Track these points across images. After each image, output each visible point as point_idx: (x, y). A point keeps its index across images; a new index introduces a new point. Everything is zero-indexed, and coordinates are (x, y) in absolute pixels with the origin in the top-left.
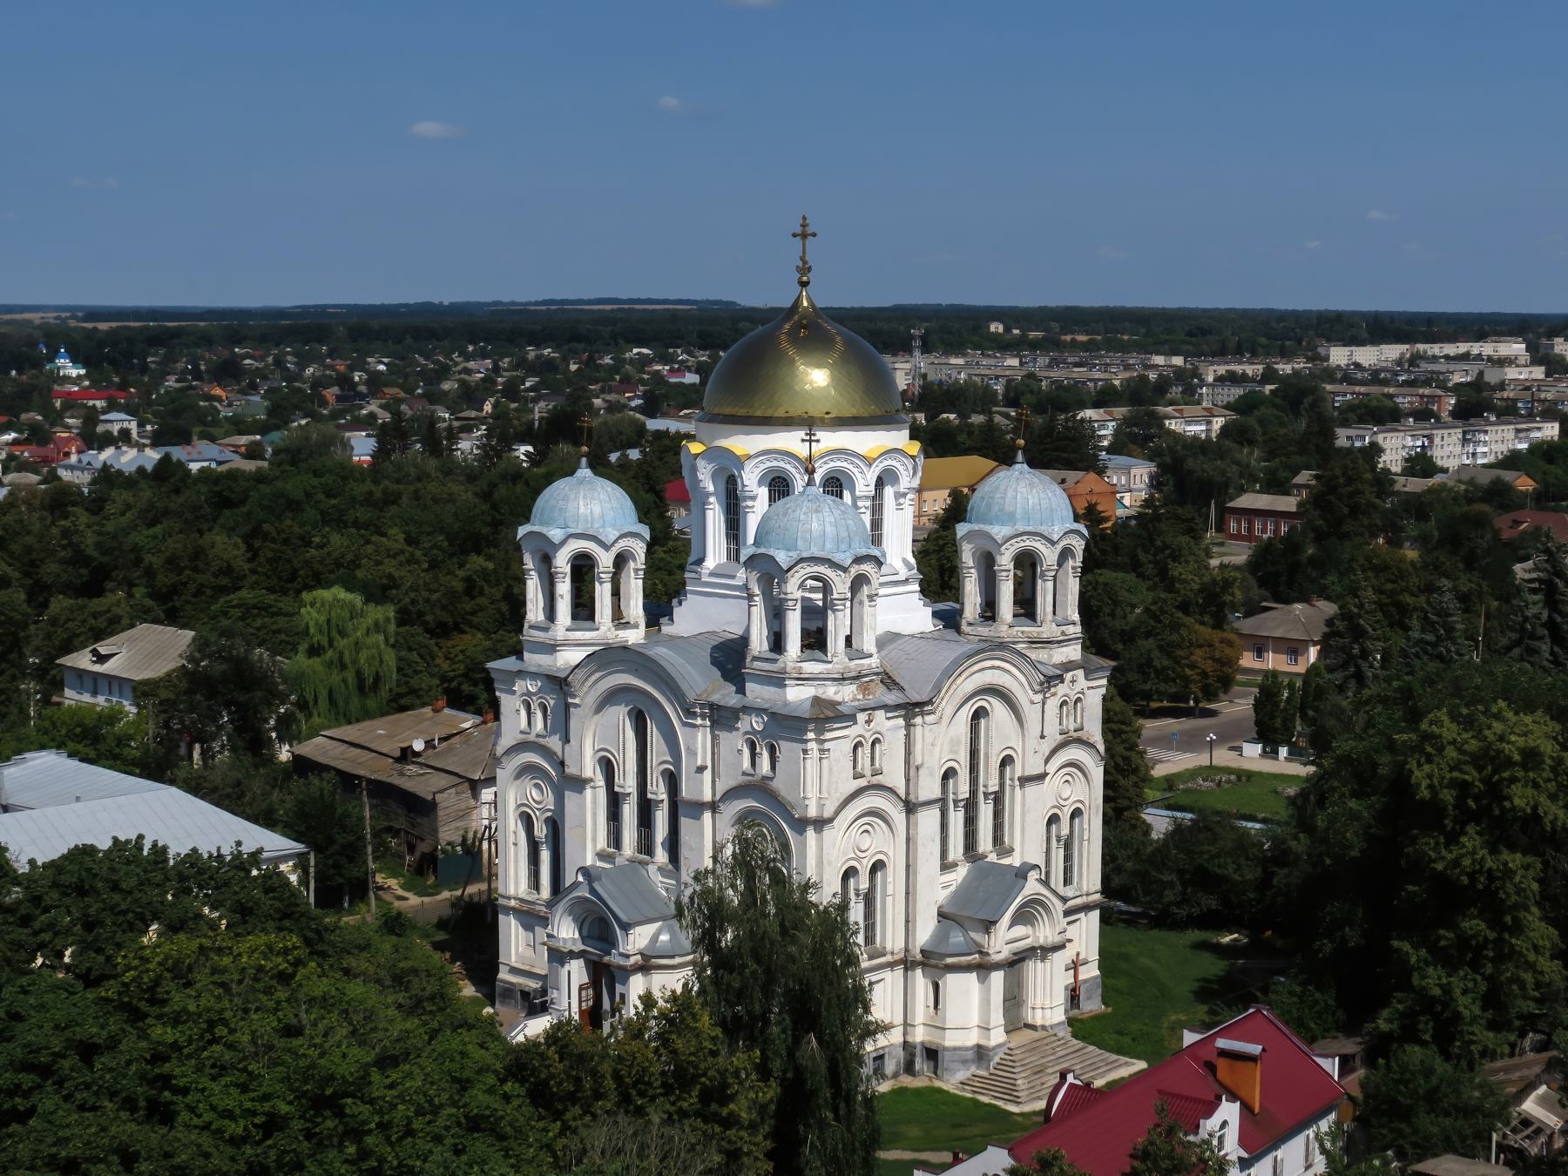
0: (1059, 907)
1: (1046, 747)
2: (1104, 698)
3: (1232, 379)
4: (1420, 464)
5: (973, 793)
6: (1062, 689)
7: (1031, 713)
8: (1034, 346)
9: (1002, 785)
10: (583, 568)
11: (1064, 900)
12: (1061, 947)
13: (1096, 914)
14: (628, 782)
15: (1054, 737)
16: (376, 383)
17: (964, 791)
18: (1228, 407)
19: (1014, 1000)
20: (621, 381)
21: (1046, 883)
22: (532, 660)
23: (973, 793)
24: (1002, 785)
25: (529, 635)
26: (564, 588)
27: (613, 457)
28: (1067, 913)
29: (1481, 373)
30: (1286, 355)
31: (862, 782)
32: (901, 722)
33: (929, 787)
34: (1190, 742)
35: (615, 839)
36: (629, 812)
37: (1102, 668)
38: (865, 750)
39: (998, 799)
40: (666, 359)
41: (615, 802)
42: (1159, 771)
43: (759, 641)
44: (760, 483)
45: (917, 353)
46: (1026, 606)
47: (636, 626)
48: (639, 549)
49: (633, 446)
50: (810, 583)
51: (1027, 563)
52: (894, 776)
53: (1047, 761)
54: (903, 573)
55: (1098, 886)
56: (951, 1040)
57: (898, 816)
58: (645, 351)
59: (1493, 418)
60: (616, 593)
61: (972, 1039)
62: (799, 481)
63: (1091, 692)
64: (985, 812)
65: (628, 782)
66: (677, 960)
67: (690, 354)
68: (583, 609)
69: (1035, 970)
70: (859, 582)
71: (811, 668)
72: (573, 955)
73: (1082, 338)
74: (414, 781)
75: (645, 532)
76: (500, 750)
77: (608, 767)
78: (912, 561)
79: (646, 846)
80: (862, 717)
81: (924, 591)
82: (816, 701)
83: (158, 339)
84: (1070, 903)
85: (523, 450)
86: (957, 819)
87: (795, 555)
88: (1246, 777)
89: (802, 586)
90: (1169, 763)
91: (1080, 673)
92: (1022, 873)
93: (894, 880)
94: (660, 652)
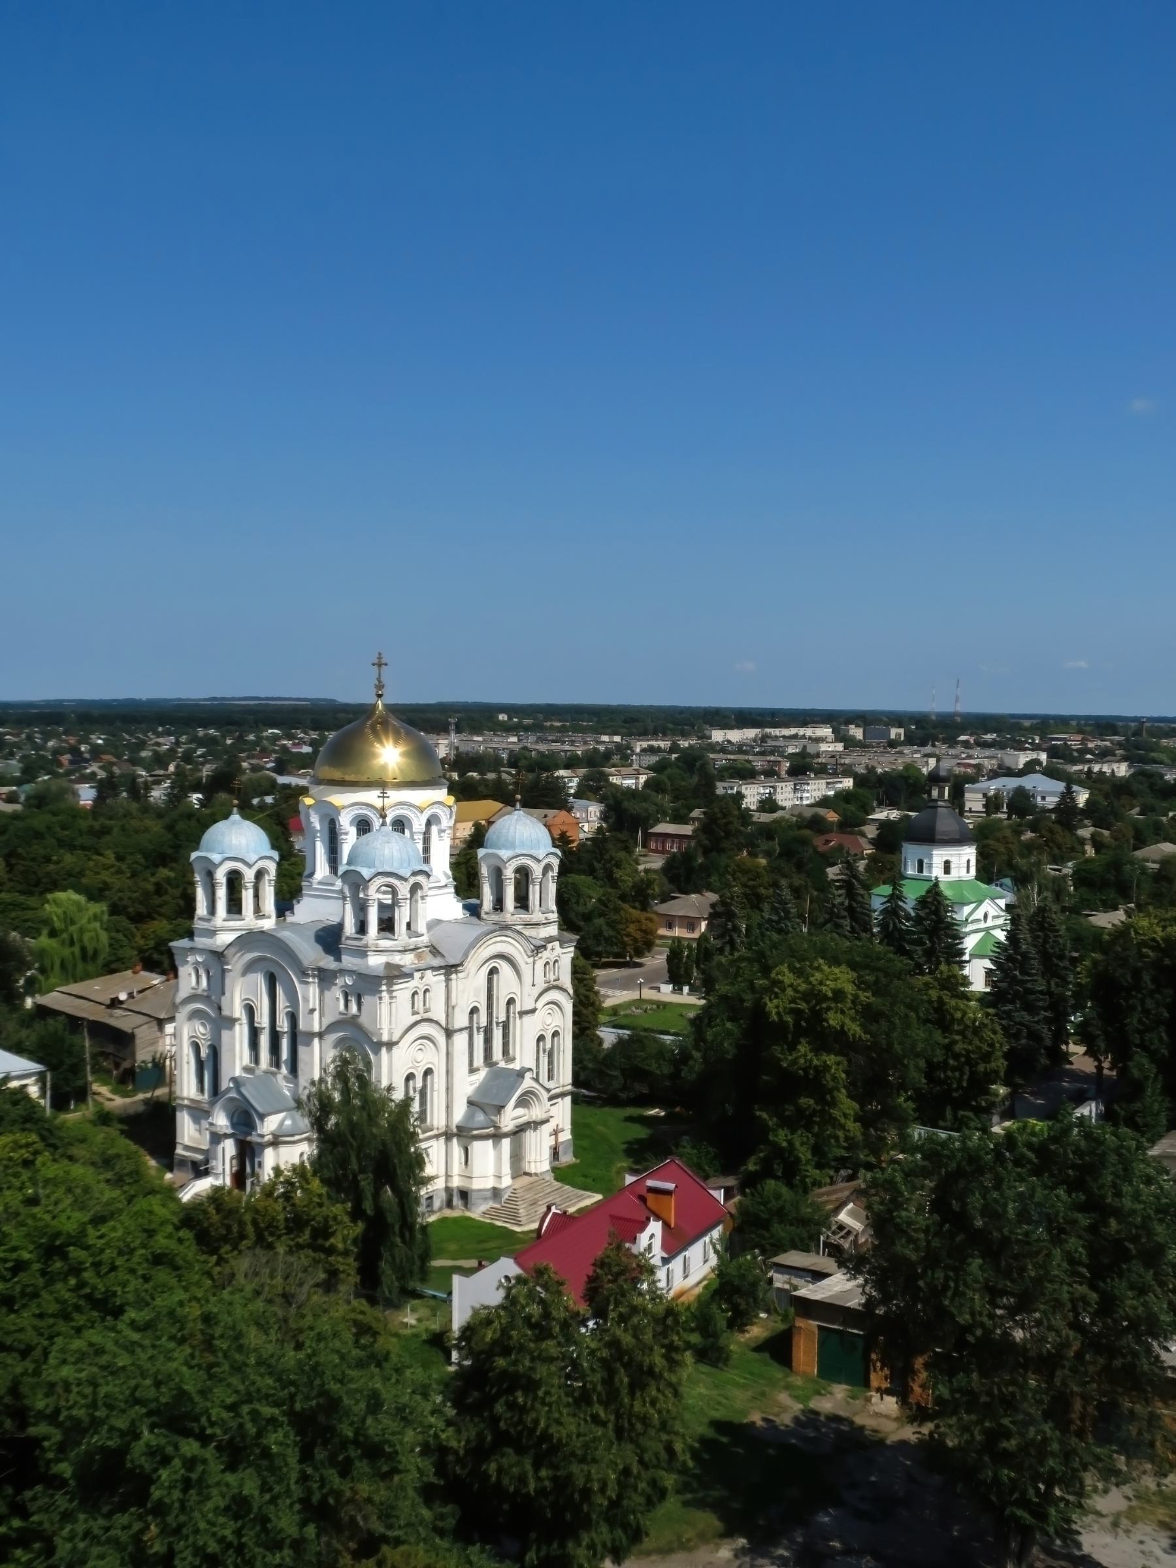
0: (545, 1095)
1: (536, 991)
2: (573, 959)
4: (768, 805)
5: (490, 1022)
6: (546, 955)
7: (526, 970)
8: (527, 729)
9: (508, 1017)
10: (234, 880)
11: (548, 1090)
12: (547, 1121)
13: (568, 1099)
14: (263, 1020)
15: (541, 985)
16: (96, 752)
17: (483, 1022)
18: (649, 768)
19: (517, 1157)
20: (261, 751)
21: (537, 1080)
22: (200, 942)
23: (490, 1022)
24: (508, 1017)
25: (198, 925)
26: (222, 893)
27: (255, 801)
28: (550, 1099)
29: (805, 747)
30: (685, 735)
31: (417, 1017)
32: (442, 978)
33: (461, 1020)
34: (626, 985)
35: (256, 1059)
36: (264, 1040)
37: (571, 941)
38: (421, 994)
39: (506, 1026)
40: (290, 737)
41: (254, 1033)
43: (350, 928)
44: (351, 823)
45: (453, 734)
46: (522, 902)
47: (269, 917)
48: (272, 867)
49: (268, 794)
50: (383, 888)
51: (523, 874)
52: (439, 1014)
53: (536, 1001)
54: (444, 881)
55: (570, 1081)
56: (476, 1185)
57: (441, 1038)
58: (276, 731)
59: (812, 775)
60: (256, 896)
61: (490, 1184)
62: (376, 822)
63: (565, 955)
64: (497, 1034)
65: (263, 1020)
66: (297, 1138)
67: (305, 733)
68: (235, 906)
69: (530, 1136)
70: (415, 888)
71: (385, 944)
72: (226, 1136)
73: (558, 724)
74: (120, 1020)
75: (276, 855)
76: (178, 1000)
77: (250, 1011)
78: (450, 873)
80: (417, 975)
81: (458, 892)
82: (388, 965)
84: (553, 1092)
85: (195, 797)
86: (479, 1039)
87: (373, 871)
88: (662, 1006)
89: (378, 891)
90: (614, 999)
91: (557, 944)
92: (521, 1074)
93: (438, 1080)
94: (285, 935)
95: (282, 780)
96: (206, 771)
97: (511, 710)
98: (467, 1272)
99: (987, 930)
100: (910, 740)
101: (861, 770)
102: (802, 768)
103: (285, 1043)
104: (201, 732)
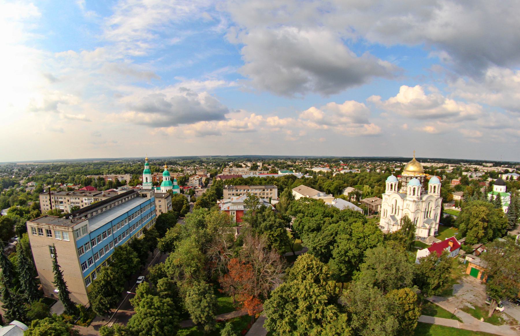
3: (452, 166)
6: (438, 201)
10: (391, 185)
17: (427, 210)
26: (390, 187)
30: (457, 164)
34: (448, 206)
39: (430, 212)
41: (393, 208)
42: (445, 209)
46: (434, 192)
51: (435, 187)
63: (440, 201)
65: (394, 207)
71: (414, 197)
79: (395, 213)
83: (350, 159)
85: (383, 172)
88: (453, 210)
90: (446, 208)
95: (396, 169)
96: (385, 168)
97: (430, 159)
98: (420, 249)
99: (506, 201)
100: (494, 166)
101: (486, 171)
102: (476, 170)
103: (397, 211)
104: (384, 162)
